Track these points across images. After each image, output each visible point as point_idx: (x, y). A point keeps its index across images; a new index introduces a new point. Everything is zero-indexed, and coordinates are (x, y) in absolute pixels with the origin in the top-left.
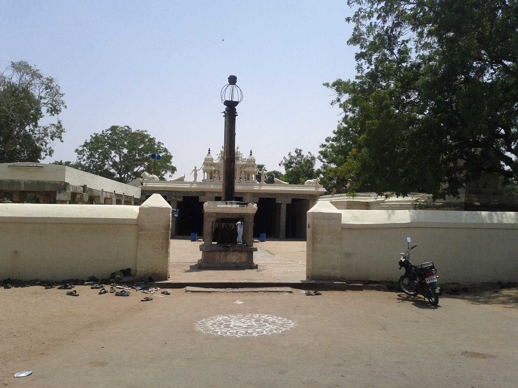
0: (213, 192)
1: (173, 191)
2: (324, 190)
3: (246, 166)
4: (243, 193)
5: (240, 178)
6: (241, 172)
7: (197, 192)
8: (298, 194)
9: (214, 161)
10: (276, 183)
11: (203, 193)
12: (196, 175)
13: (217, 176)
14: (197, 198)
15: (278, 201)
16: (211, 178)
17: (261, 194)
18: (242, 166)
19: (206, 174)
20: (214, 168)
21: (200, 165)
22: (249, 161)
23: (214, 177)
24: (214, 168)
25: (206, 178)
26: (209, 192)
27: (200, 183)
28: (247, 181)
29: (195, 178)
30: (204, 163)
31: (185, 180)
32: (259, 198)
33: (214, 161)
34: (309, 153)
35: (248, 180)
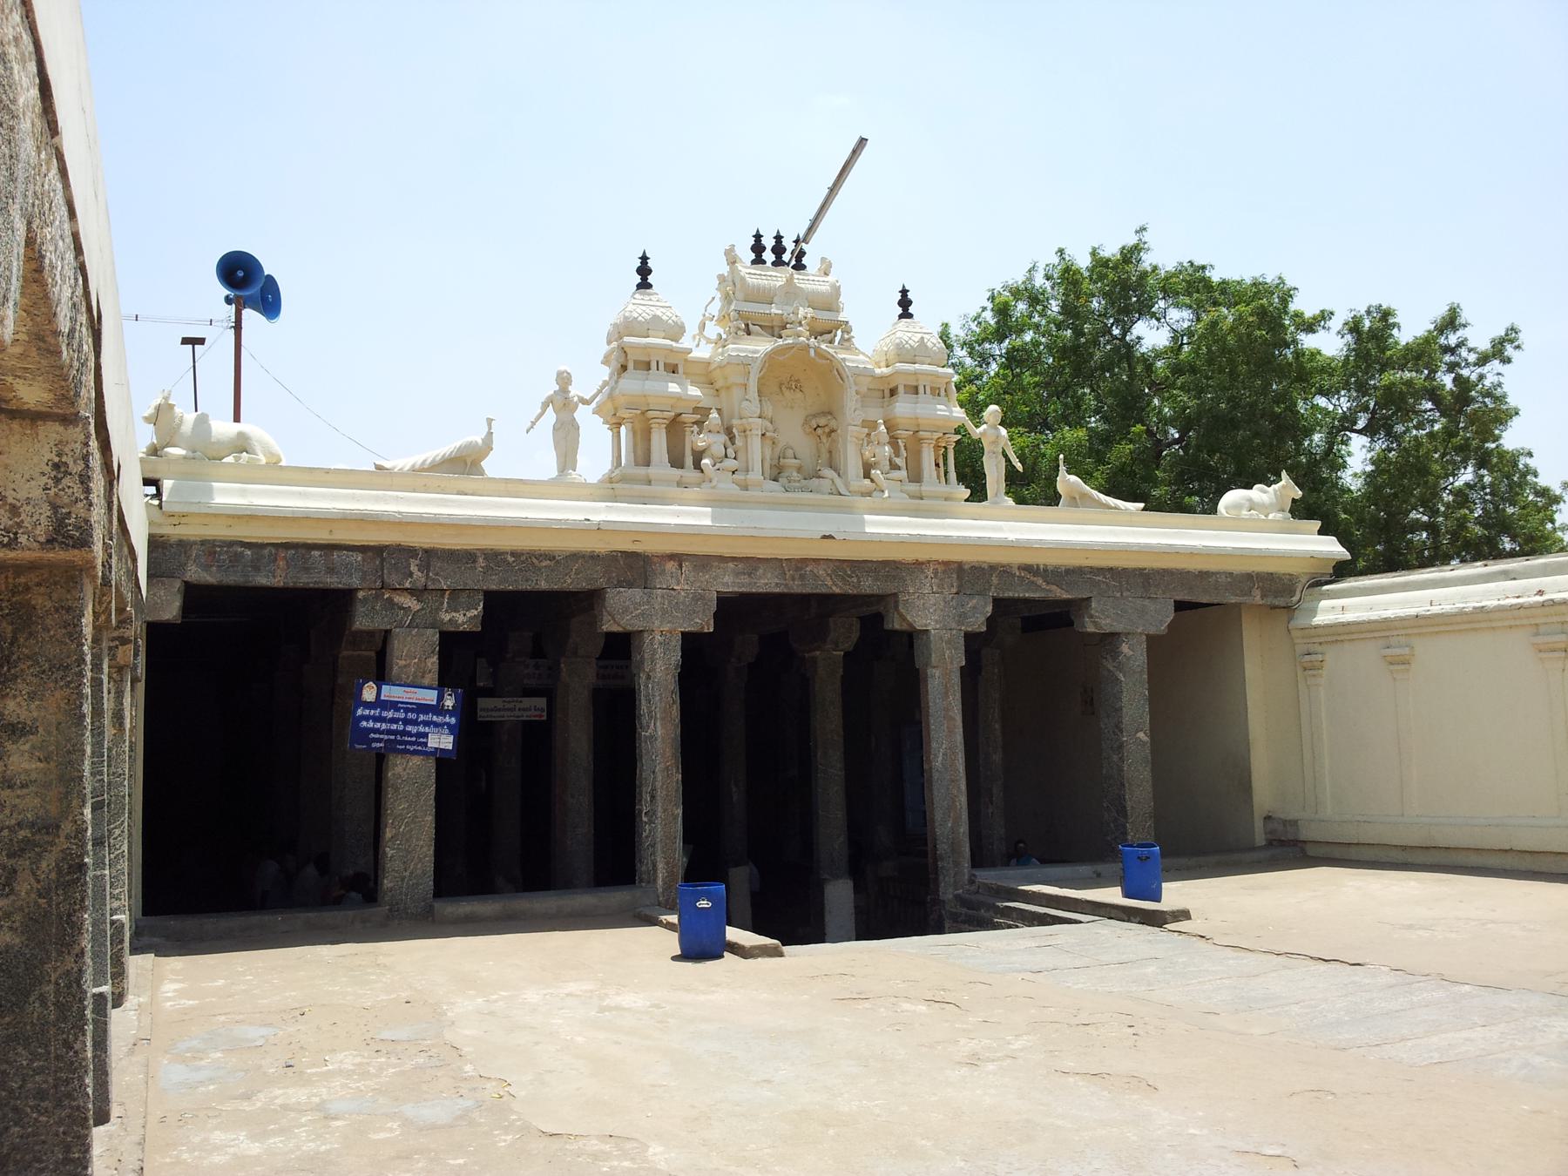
0: (704, 562)
1: (403, 553)
2: (1332, 547)
4: (892, 569)
7: (594, 557)
8: (1203, 575)
9: (686, 342)
11: (636, 566)
12: (567, 439)
13: (718, 450)
14: (588, 601)
15: (1101, 618)
17: (1003, 571)
20: (694, 391)
22: (904, 354)
24: (694, 391)
26: (678, 558)
28: (913, 487)
31: (492, 466)
32: (997, 602)
33: (686, 342)
35: (916, 477)
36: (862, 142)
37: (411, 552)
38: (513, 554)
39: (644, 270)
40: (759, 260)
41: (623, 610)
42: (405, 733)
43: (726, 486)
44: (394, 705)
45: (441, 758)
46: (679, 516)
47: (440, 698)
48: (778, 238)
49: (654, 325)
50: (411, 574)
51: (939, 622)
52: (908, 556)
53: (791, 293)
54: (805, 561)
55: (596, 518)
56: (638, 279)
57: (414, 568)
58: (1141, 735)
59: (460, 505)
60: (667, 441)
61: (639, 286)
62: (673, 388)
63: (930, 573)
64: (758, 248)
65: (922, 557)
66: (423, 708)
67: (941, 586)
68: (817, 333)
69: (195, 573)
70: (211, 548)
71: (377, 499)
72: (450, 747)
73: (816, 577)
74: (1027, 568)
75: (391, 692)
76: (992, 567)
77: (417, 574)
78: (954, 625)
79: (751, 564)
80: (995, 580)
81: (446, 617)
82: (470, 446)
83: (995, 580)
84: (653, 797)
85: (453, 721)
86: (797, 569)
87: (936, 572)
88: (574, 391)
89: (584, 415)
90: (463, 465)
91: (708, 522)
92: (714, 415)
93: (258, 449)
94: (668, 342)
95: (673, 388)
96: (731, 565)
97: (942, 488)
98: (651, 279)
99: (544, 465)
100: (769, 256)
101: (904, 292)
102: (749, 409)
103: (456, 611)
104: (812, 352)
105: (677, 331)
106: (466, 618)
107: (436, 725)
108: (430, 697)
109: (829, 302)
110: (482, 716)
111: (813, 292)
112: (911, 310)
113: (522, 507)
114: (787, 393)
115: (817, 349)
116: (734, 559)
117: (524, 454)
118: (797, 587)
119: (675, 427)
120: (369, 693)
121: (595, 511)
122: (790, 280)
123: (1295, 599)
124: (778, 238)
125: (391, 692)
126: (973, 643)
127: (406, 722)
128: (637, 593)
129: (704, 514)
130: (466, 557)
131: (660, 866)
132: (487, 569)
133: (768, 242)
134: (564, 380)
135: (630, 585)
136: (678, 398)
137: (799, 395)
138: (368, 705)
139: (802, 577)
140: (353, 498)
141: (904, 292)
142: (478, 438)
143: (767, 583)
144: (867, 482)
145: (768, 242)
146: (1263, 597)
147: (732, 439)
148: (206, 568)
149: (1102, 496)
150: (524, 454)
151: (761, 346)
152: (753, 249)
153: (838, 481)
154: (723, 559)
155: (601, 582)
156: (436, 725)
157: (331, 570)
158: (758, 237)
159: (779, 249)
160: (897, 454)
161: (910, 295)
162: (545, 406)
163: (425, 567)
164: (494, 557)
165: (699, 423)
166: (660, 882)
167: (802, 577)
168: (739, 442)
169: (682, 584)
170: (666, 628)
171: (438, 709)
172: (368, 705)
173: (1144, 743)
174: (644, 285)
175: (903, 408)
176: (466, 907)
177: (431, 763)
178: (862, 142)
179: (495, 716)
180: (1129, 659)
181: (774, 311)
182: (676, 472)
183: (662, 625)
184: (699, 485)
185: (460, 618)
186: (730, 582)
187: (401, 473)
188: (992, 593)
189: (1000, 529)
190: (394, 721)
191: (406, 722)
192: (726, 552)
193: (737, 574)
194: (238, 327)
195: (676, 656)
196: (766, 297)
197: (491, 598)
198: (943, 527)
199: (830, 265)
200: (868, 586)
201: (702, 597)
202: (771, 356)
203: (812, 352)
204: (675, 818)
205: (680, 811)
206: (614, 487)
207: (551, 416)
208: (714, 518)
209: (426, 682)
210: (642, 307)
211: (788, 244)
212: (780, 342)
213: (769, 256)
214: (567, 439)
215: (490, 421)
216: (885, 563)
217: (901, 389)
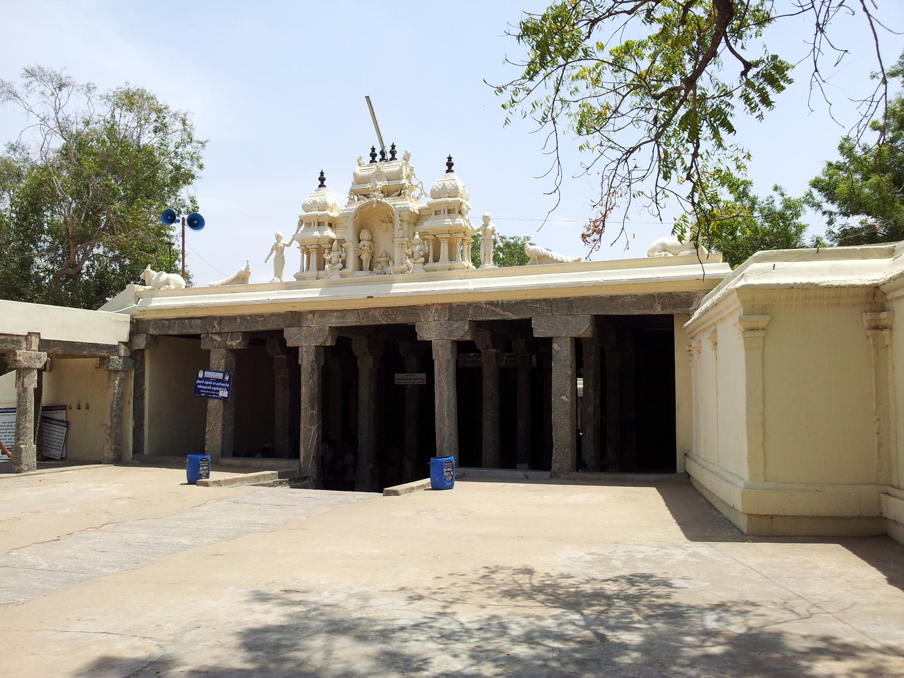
0: (324, 313)
4: (414, 310)
7: (279, 315)
8: (613, 298)
10: (534, 263)
11: (296, 317)
14: (277, 335)
16: (321, 266)
17: (476, 306)
18: (417, 219)
21: (289, 229)
27: (288, 286)
29: (279, 271)
34: (776, 189)
36: (367, 97)
37: (214, 318)
38: (250, 316)
39: (322, 179)
40: (373, 161)
41: (292, 337)
42: (212, 390)
43: (336, 277)
44: (208, 379)
52: (422, 302)
53: (379, 175)
54: (369, 309)
55: (271, 298)
56: (319, 183)
58: (564, 398)
59: (233, 297)
60: (318, 256)
63: (433, 311)
64: (373, 155)
65: (429, 302)
66: (218, 380)
67: (439, 317)
68: (387, 193)
69: (152, 331)
70: (158, 322)
71: (199, 298)
73: (374, 316)
74: (491, 303)
75: (208, 374)
76: (469, 305)
78: (446, 337)
79: (344, 312)
80: (471, 311)
81: (229, 343)
82: (240, 272)
83: (471, 311)
86: (366, 313)
87: (437, 310)
90: (241, 279)
91: (317, 295)
93: (171, 282)
97: (448, 264)
98: (325, 183)
100: (379, 157)
101: (450, 158)
102: (349, 235)
106: (235, 343)
108: (220, 376)
110: (397, 382)
111: (390, 173)
112: (453, 168)
113: (256, 296)
114: (384, 225)
116: (337, 311)
117: (262, 274)
118: (365, 322)
119: (320, 250)
120: (201, 375)
121: (274, 295)
123: (691, 309)
125: (208, 374)
127: (212, 386)
128: (295, 330)
132: (241, 323)
134: (278, 237)
136: (316, 237)
137: (389, 224)
138: (201, 379)
139: (368, 317)
140: (192, 299)
141: (450, 158)
143: (351, 321)
146: (662, 309)
148: (155, 329)
150: (262, 274)
151: (355, 206)
154: (332, 311)
155: (282, 326)
157: (191, 327)
158: (373, 149)
159: (383, 153)
161: (453, 161)
162: (273, 250)
163: (220, 324)
164: (243, 317)
166: (302, 458)
167: (368, 317)
169: (314, 324)
171: (222, 381)
172: (201, 379)
173: (566, 403)
174: (322, 185)
176: (229, 461)
177: (222, 401)
178: (367, 97)
179: (403, 382)
180: (557, 352)
181: (368, 186)
183: (307, 342)
185: (234, 344)
186: (335, 322)
187: (217, 286)
189: (468, 283)
190: (209, 385)
191: (212, 386)
192: (331, 308)
193: (338, 318)
194: (183, 236)
195: (312, 357)
197: (245, 334)
200: (400, 319)
201: (322, 330)
204: (310, 430)
205: (314, 428)
206: (301, 281)
213: (379, 157)
216: (409, 307)
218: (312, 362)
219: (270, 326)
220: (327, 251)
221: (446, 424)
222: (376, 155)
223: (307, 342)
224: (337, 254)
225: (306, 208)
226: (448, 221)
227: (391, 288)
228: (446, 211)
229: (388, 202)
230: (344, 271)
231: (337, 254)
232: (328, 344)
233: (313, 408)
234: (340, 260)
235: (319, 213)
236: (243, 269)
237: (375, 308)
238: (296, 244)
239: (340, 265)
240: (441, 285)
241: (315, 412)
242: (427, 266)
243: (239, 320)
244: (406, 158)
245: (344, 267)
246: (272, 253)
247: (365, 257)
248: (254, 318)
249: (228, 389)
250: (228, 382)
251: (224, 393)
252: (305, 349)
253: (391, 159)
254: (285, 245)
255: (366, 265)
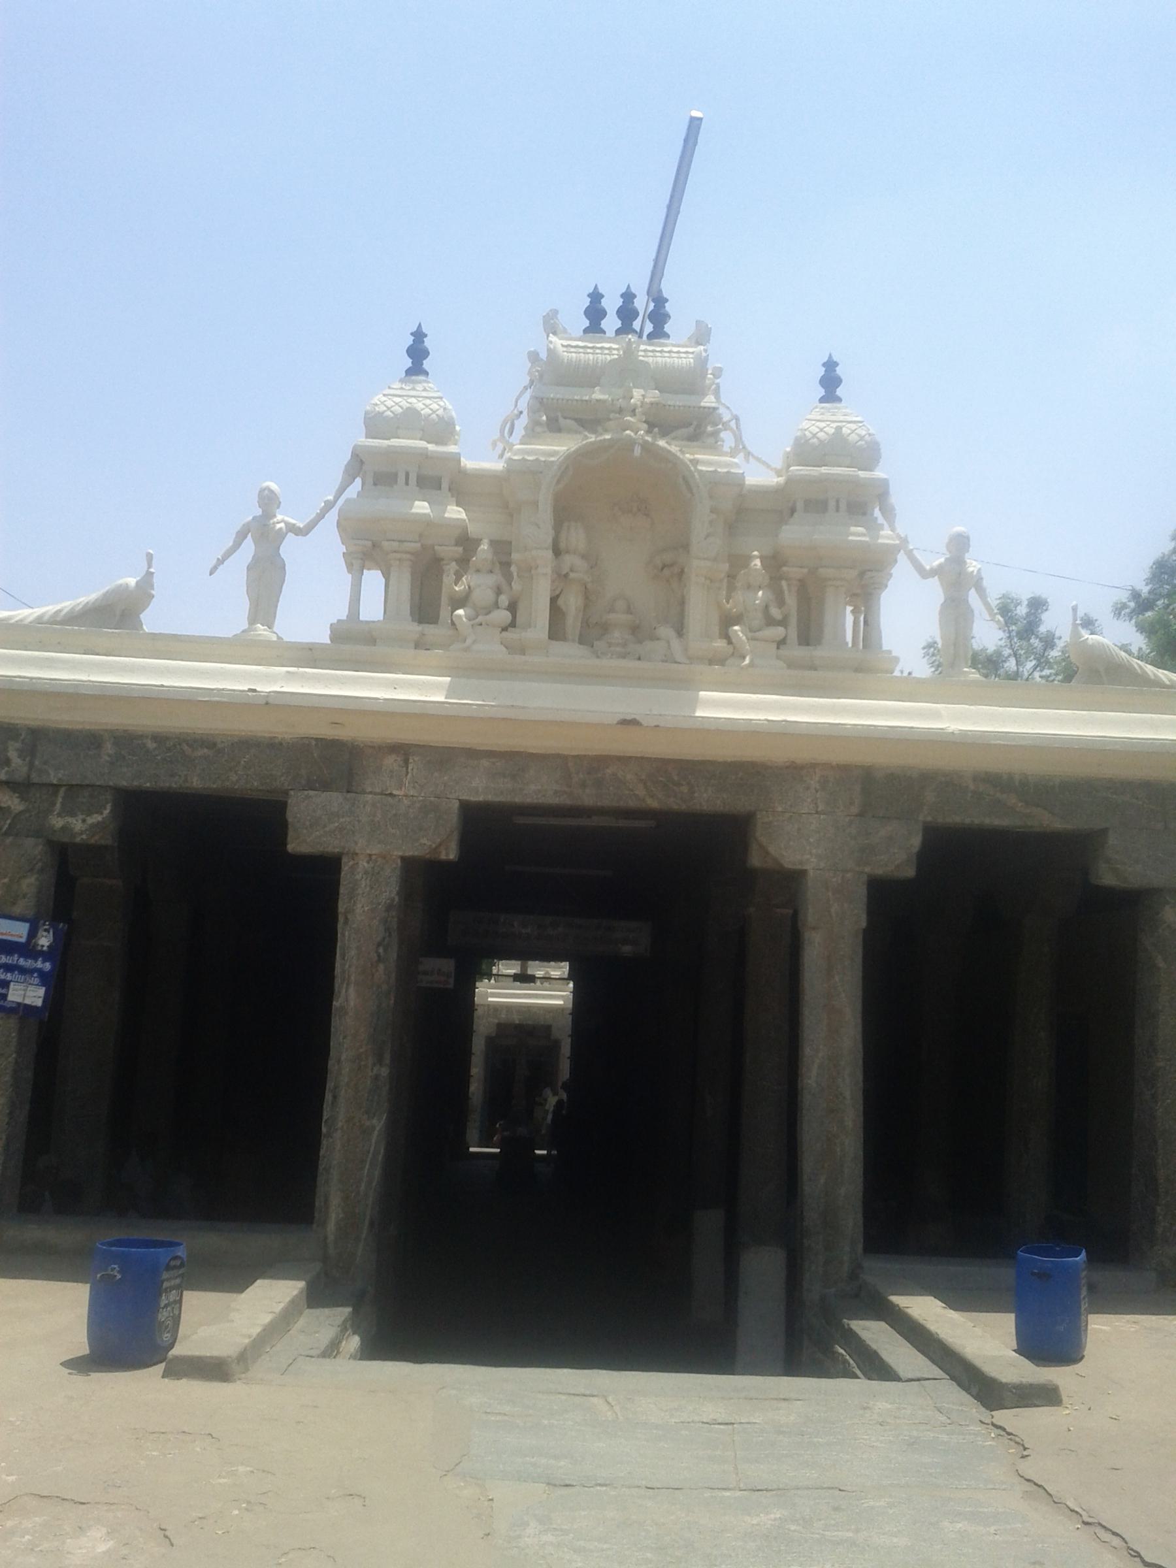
0: (443, 758)
3: (785, 504)
5: (728, 620)
6: (738, 562)
7: (273, 747)
11: (338, 758)
19: (373, 580)
20: (455, 512)
21: (312, 482)
23: (460, 601)
24: (455, 512)
25: (373, 609)
26: (403, 751)
27: (308, 656)
28: (796, 652)
29: (264, 603)
30: (358, 463)
31: (152, 621)
35: (809, 633)
43: (490, 647)
45: (24, 1011)
46: (414, 689)
47: (32, 934)
48: (628, 296)
49: (409, 421)
50: (8, 762)
51: (823, 859)
52: (778, 755)
53: (628, 370)
55: (265, 688)
56: (408, 363)
57: (12, 754)
61: (410, 372)
62: (421, 507)
64: (595, 313)
65: (803, 755)
72: (39, 1003)
77: (16, 760)
79: (516, 762)
81: (57, 822)
84: (335, 1097)
85: (47, 966)
88: (281, 518)
89: (290, 549)
90: (114, 617)
91: (442, 699)
92: (484, 546)
94: (431, 447)
95: (421, 507)
96: (485, 763)
99: (228, 615)
100: (611, 323)
102: (535, 534)
103: (73, 814)
104: (637, 451)
105: (442, 430)
106: (84, 824)
107: (23, 971)
108: (18, 931)
109: (691, 381)
115: (647, 448)
116: (491, 754)
118: (588, 798)
122: (629, 352)
124: (628, 296)
126: (883, 895)
128: (334, 800)
129: (436, 687)
130: (91, 741)
131: (335, 1201)
133: (611, 304)
134: (268, 501)
135: (326, 786)
136: (426, 523)
142: (132, 582)
143: (539, 789)
144: (720, 644)
145: (611, 304)
147: (509, 578)
149: (1149, 669)
151: (559, 448)
152: (587, 313)
153: (676, 644)
154: (472, 754)
156: (23, 971)
160: (781, 602)
162: (241, 536)
164: (128, 742)
165: (464, 563)
166: (331, 1227)
168: (516, 586)
170: (375, 849)
171: (27, 949)
175: (793, 534)
181: (598, 395)
182: (416, 628)
184: (444, 646)
186: (481, 788)
188: (925, 816)
189: (937, 715)
195: (390, 891)
196: (588, 376)
198: (833, 710)
199: (708, 331)
200: (707, 799)
202: (575, 461)
203: (637, 451)
205: (378, 1124)
207: (248, 548)
208: (451, 691)
209: (17, 910)
210: (392, 397)
211: (641, 303)
212: (592, 438)
213: (611, 323)
214: (266, 582)
215: (150, 558)
217: (800, 505)
218: (389, 908)
219: (240, 780)
220: (454, 566)
221: (849, 1123)
222: (603, 314)
223: (372, 850)
224: (491, 580)
225: (375, 424)
226: (857, 534)
227: (694, 703)
228: (843, 506)
229: (674, 449)
230: (511, 635)
231: (491, 580)
232: (451, 854)
233: (380, 1060)
234: (504, 600)
235: (431, 447)
236: (132, 582)
237: (623, 760)
238: (329, 530)
239: (503, 616)
240: (858, 712)
241: (385, 1072)
242: (784, 652)
243: (109, 748)
244: (702, 336)
245: (513, 624)
246: (237, 545)
247: (572, 602)
248: (174, 747)
249: (44, 978)
250: (46, 956)
251: (29, 993)
252: (363, 864)
253: (650, 336)
254: (292, 529)
255: (572, 622)
